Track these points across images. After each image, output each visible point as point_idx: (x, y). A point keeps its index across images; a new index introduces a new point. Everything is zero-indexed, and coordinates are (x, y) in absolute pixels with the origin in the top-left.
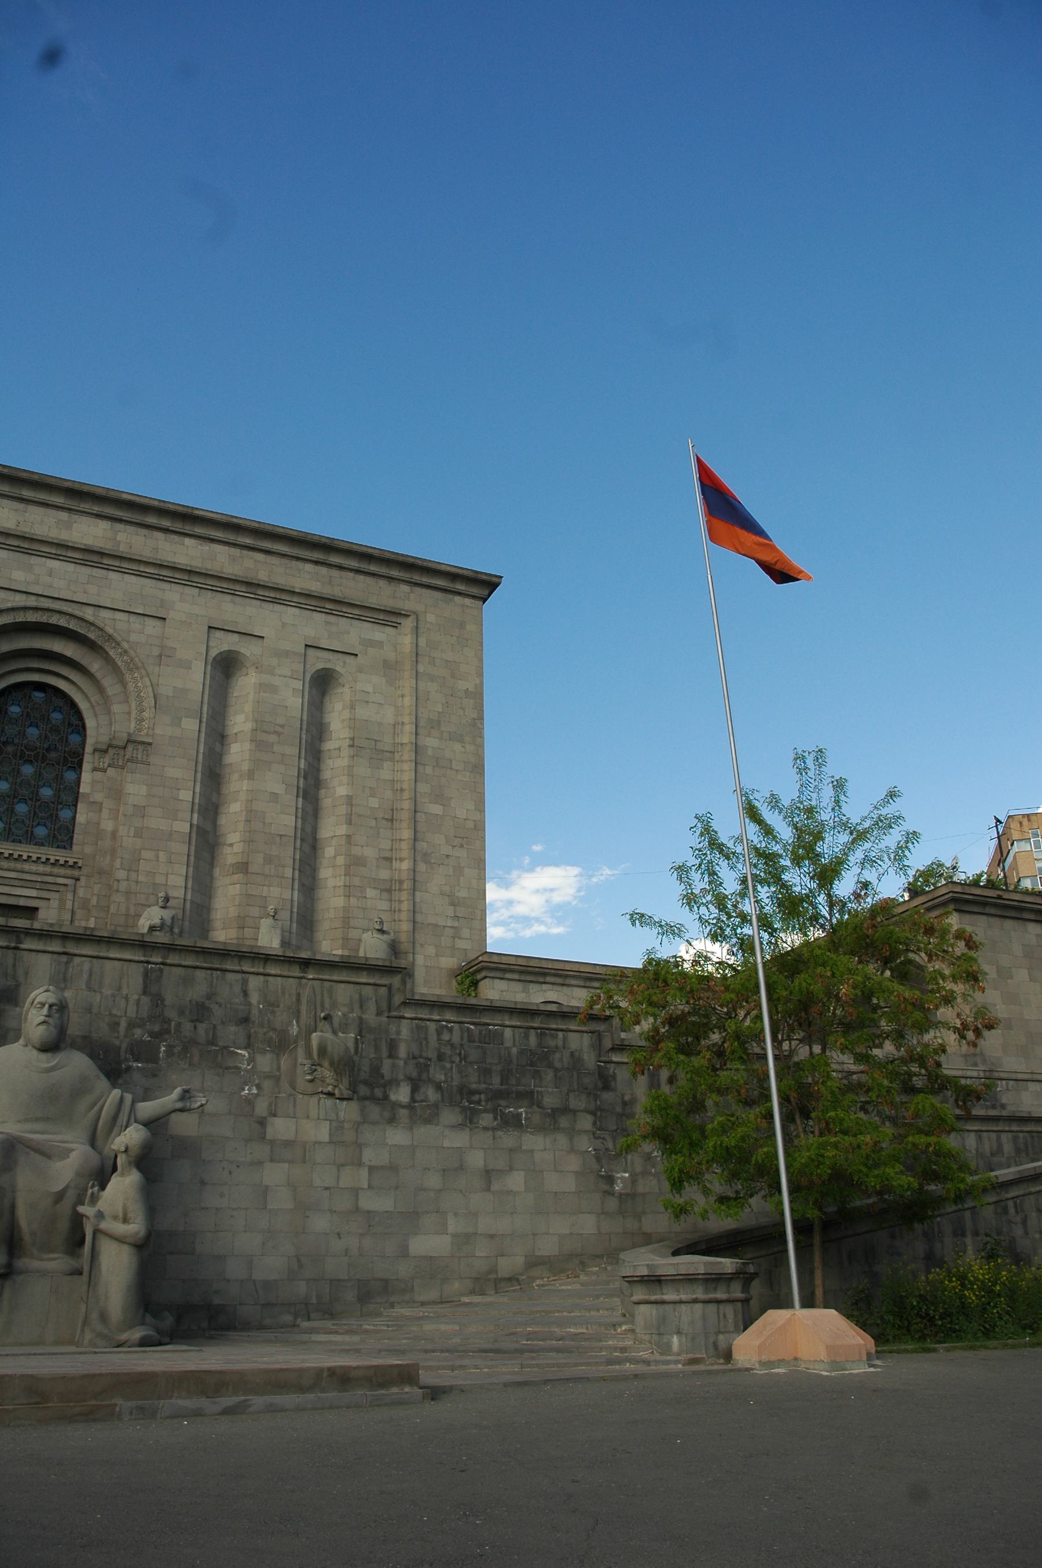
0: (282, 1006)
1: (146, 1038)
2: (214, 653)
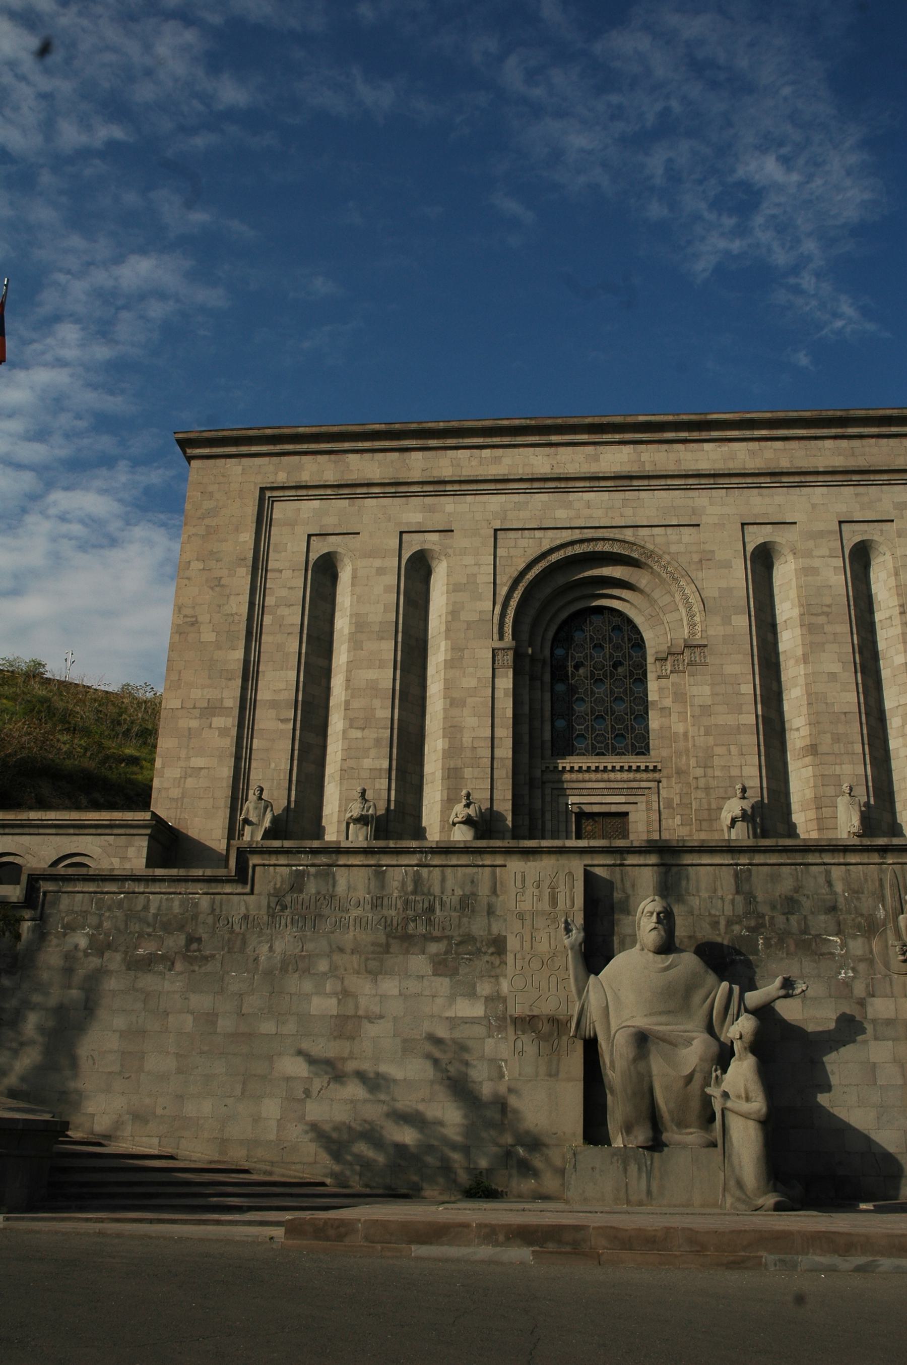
0: (866, 892)
1: (744, 932)
2: (750, 548)
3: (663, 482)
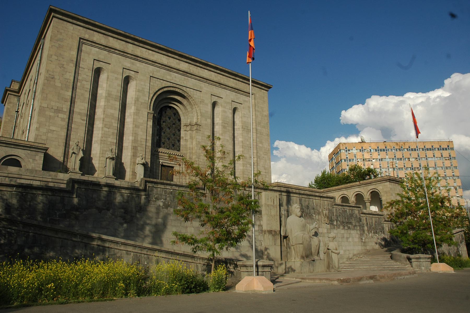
3: (194, 77)
